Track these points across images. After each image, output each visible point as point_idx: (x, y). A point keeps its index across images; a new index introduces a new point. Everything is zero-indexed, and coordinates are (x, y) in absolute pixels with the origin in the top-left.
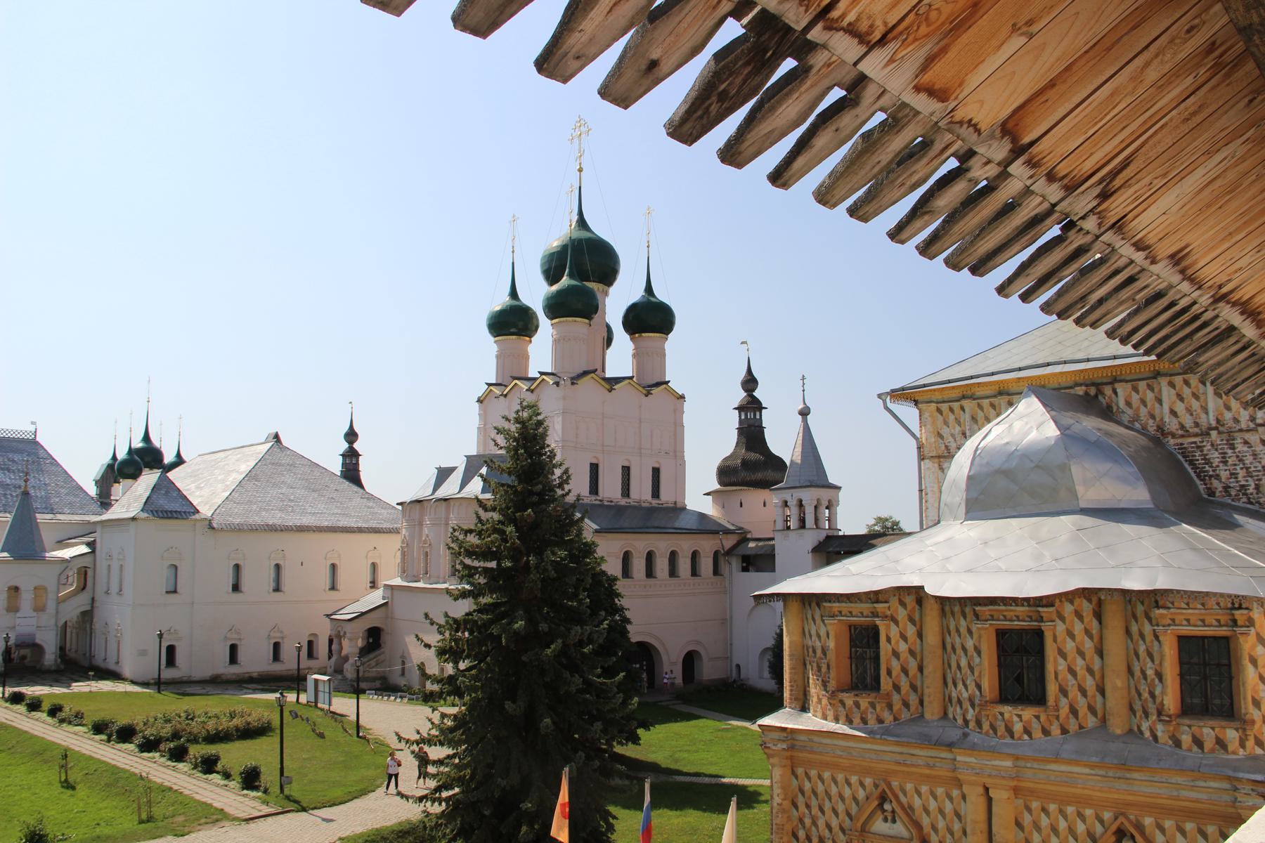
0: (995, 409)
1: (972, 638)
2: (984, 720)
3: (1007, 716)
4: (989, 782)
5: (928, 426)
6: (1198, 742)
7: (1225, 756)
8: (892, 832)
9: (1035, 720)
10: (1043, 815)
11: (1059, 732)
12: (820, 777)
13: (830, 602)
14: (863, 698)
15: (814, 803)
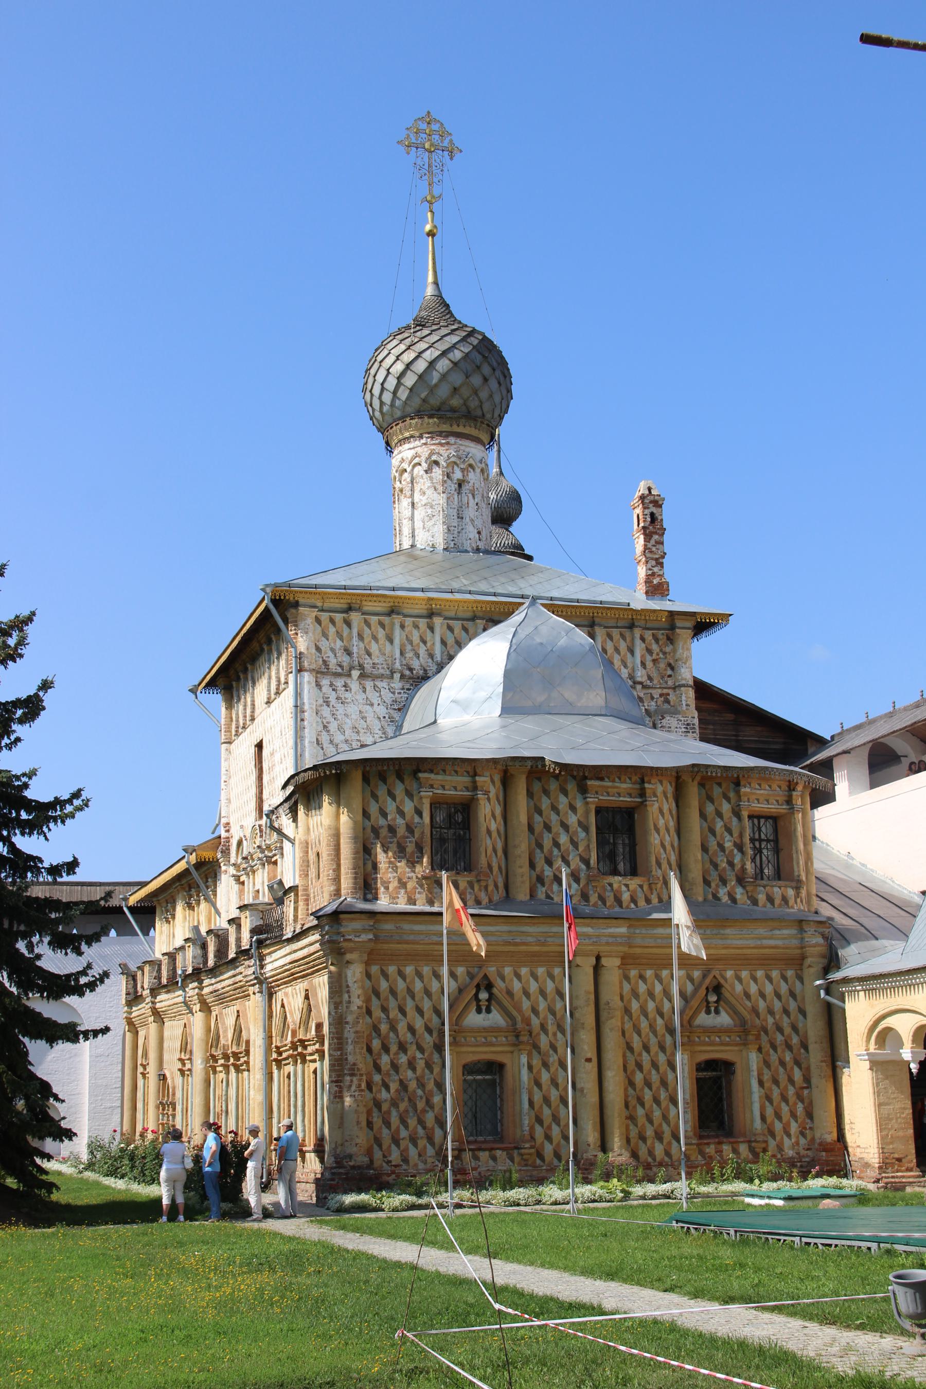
0: (384, 629)
1: (576, 814)
2: (591, 892)
3: (615, 886)
4: (603, 949)
5: (310, 634)
6: (770, 899)
7: (788, 910)
8: (487, 1023)
9: (639, 889)
10: (640, 981)
11: (657, 900)
12: (401, 974)
13: (431, 771)
14: (465, 876)
15: (392, 1004)
